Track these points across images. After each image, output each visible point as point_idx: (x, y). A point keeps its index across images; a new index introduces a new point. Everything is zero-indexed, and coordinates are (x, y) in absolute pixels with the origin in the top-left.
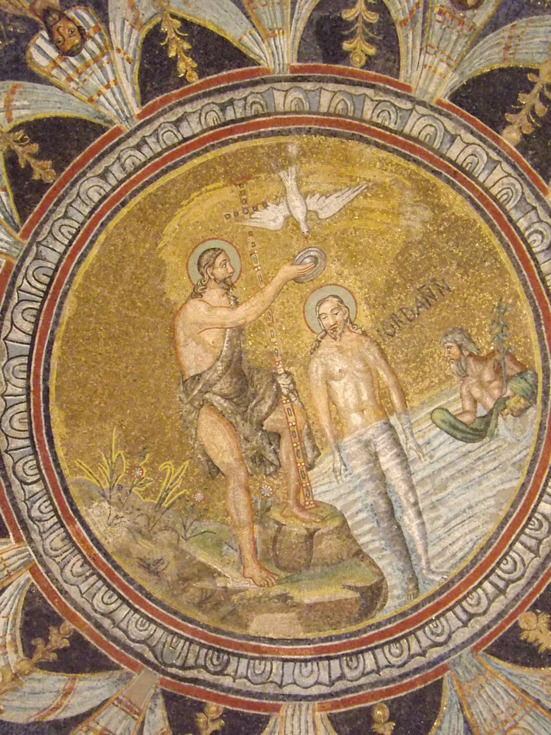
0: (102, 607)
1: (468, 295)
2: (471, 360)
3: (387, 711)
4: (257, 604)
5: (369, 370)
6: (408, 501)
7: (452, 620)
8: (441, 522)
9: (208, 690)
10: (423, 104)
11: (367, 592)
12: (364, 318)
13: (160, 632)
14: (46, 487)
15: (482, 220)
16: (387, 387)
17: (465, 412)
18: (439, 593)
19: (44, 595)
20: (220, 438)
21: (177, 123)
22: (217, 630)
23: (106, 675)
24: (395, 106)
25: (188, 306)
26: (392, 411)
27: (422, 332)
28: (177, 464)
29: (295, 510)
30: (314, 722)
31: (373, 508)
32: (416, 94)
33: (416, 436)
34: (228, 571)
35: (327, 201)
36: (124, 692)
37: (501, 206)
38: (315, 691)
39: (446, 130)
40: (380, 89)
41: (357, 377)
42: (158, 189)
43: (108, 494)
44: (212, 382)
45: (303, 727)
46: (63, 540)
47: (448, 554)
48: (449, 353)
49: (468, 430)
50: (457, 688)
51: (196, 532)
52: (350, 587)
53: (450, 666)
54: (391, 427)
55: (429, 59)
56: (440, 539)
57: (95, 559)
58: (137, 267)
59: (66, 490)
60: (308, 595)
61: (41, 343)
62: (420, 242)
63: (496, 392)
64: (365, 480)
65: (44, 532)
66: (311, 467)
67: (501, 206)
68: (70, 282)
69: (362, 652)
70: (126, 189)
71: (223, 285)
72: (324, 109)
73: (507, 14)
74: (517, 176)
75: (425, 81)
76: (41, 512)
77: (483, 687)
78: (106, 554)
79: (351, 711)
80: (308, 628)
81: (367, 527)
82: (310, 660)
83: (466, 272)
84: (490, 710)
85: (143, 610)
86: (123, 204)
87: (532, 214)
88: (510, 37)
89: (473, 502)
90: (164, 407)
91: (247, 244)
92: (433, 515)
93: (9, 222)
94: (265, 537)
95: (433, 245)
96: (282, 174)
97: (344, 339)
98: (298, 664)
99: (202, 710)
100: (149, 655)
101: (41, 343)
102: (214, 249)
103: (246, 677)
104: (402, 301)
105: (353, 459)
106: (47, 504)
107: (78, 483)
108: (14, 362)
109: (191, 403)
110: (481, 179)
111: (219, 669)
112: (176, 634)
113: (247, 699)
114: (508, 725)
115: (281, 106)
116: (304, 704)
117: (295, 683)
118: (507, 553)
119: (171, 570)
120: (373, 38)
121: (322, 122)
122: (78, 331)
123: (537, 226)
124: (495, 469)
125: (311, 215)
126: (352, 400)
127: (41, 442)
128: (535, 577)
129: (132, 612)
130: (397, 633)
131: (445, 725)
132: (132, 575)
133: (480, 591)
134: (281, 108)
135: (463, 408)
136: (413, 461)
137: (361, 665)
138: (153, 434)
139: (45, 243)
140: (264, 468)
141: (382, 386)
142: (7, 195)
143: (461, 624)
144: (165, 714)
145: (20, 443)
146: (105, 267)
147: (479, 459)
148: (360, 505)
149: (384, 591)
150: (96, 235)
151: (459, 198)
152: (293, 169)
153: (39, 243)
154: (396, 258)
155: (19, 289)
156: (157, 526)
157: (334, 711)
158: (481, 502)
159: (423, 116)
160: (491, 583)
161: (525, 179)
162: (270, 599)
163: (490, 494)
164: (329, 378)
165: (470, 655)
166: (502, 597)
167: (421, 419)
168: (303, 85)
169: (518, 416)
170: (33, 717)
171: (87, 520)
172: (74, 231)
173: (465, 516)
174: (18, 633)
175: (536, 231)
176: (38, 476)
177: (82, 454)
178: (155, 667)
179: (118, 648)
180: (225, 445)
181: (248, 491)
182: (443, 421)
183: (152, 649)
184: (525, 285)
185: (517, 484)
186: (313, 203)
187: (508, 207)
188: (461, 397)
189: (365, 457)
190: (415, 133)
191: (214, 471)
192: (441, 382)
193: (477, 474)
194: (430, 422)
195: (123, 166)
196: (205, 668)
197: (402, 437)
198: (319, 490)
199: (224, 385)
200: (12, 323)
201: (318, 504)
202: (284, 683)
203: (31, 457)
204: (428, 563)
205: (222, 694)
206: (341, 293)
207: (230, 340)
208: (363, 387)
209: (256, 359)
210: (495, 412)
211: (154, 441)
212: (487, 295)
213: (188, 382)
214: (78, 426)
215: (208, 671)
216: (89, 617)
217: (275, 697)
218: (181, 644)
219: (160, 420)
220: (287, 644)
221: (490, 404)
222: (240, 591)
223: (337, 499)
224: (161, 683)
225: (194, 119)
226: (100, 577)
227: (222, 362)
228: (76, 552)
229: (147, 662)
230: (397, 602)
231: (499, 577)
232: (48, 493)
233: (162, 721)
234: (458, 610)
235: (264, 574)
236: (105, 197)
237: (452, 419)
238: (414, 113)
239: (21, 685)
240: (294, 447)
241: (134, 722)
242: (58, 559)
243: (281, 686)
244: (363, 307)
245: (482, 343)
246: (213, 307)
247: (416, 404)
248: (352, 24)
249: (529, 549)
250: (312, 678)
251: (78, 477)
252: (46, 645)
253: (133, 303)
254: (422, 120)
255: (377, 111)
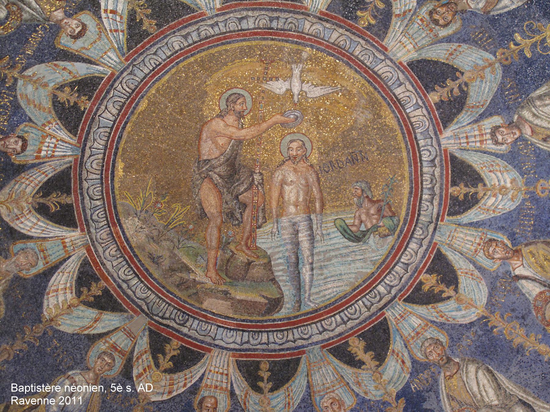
0: (123, 277)
1: (377, 166)
2: (366, 200)
3: (268, 366)
4: (210, 293)
5: (308, 186)
6: (308, 261)
7: (314, 329)
8: (323, 277)
9: (174, 332)
10: (391, 60)
11: (272, 301)
12: (314, 158)
13: (153, 296)
14: (104, 204)
15: (400, 132)
16: (315, 198)
17: (353, 225)
18: (311, 313)
19: (92, 264)
20: (212, 198)
21: (241, 20)
22: (185, 302)
23: (119, 314)
24: (374, 55)
25: (213, 121)
26: (314, 211)
27: (344, 176)
28: (183, 206)
29: (244, 248)
30: (228, 362)
31: (288, 259)
32: (390, 54)
33: (323, 229)
34: (199, 271)
35: (315, 89)
36: (128, 326)
37: (413, 129)
38: (232, 346)
39: (398, 77)
40: (369, 42)
41: (300, 188)
42: (216, 52)
43: (139, 214)
44: (215, 166)
45: (222, 364)
46: (107, 235)
47: (321, 294)
48: (356, 191)
49: (353, 235)
50: (308, 364)
51: (185, 246)
52: (263, 296)
53: (306, 352)
54: (311, 219)
55: (404, 40)
56: (319, 285)
57: (124, 248)
58: (189, 92)
59: (115, 207)
60: (240, 296)
61: (120, 122)
62: (360, 129)
63: (374, 221)
64: (287, 243)
65: (98, 229)
66: (260, 227)
67: (413, 129)
68: (146, 92)
69: (262, 332)
70: (196, 48)
71: (237, 115)
72: (332, 41)
73: (459, 38)
74: (429, 118)
75: (397, 49)
76: (99, 217)
77: (321, 368)
78: (131, 247)
79: (249, 361)
80: (235, 312)
81: (281, 268)
82: (233, 329)
83: (380, 154)
84: (322, 380)
85: (146, 282)
86: (192, 55)
87: (429, 141)
88: (455, 50)
89: (343, 273)
90: (183, 173)
91: (259, 96)
92: (319, 272)
93: (120, 51)
94: (223, 258)
95: (367, 133)
96: (293, 66)
97: (299, 165)
98: (226, 330)
99: (169, 344)
100: (145, 307)
101: (120, 122)
102: (239, 94)
103: (196, 330)
104: (339, 156)
105: (284, 230)
106: (102, 213)
107: (123, 205)
108: (101, 130)
109: (200, 174)
110: (408, 111)
111: (182, 322)
112: (162, 298)
113: (194, 342)
114: (330, 390)
115: (307, 30)
116: (225, 352)
117: (222, 340)
118: (353, 304)
119: (166, 263)
120: (376, 16)
121: (327, 46)
122: (144, 119)
123: (429, 147)
124: (360, 260)
125: (302, 93)
126: (293, 199)
127: (107, 178)
128: (364, 321)
129: (140, 282)
130: (283, 327)
131: (297, 381)
132: (143, 262)
133: (333, 318)
134: (306, 31)
135: (354, 223)
136: (317, 241)
137: (260, 338)
138: (173, 187)
139: (138, 66)
140: (232, 221)
141: (312, 197)
142: (124, 35)
143: (318, 332)
144: (148, 341)
145: (94, 176)
146: (171, 88)
147: (354, 251)
148: (281, 255)
149: (281, 303)
150: (170, 69)
151: (392, 115)
152: (301, 65)
153: (135, 65)
154: (344, 132)
155: (115, 89)
156: (163, 237)
157: (240, 359)
158: (348, 274)
159: (388, 66)
160: (340, 316)
161: (432, 121)
162: (218, 291)
163: (353, 271)
164: (283, 182)
165: (319, 350)
166: (344, 326)
167: (329, 220)
168: (324, 23)
169: (382, 238)
170: (76, 330)
171: (124, 226)
172: (158, 63)
173: (336, 278)
174: (74, 283)
175: (428, 150)
176: (101, 197)
177: (129, 189)
178: (147, 314)
179: (128, 301)
180: (213, 202)
181: (220, 230)
182: (341, 226)
183: (147, 304)
184: (411, 174)
185: (369, 271)
186: (305, 87)
187: (417, 131)
188: (354, 217)
189: (291, 230)
190: (380, 72)
191: (203, 215)
192: (346, 206)
193: (351, 259)
194: (333, 224)
195: (199, 34)
196: (174, 320)
197: (315, 227)
198: (260, 241)
199: (222, 170)
200: (106, 108)
201: (257, 248)
202: (216, 338)
203: (99, 185)
204: (309, 296)
205: (182, 337)
206: (305, 139)
207: (233, 146)
208: (301, 194)
209: (244, 161)
210: (370, 231)
211: (173, 190)
212: (388, 171)
213: (201, 162)
214: (130, 173)
215: (176, 323)
216: (115, 281)
217: (210, 344)
218: (164, 305)
219: (180, 179)
220: (222, 318)
221: (369, 226)
222: (203, 283)
223: (269, 249)
224: (149, 324)
225: (251, 21)
226: (125, 260)
227: (224, 157)
228: (114, 243)
229: (143, 311)
230: (287, 311)
231: (345, 314)
232: (105, 207)
233: (146, 345)
234: (319, 325)
235: (218, 278)
236: (181, 49)
237: (346, 227)
238: (384, 62)
239: (72, 312)
240: (252, 214)
241: (131, 342)
242: (103, 245)
243: (214, 339)
244: (315, 151)
245: (376, 193)
246: (228, 125)
247: (328, 212)
248: (368, 4)
249: (366, 306)
250: (232, 339)
251: (124, 201)
252: (88, 292)
253: (181, 111)
254: (387, 68)
255: (362, 53)
